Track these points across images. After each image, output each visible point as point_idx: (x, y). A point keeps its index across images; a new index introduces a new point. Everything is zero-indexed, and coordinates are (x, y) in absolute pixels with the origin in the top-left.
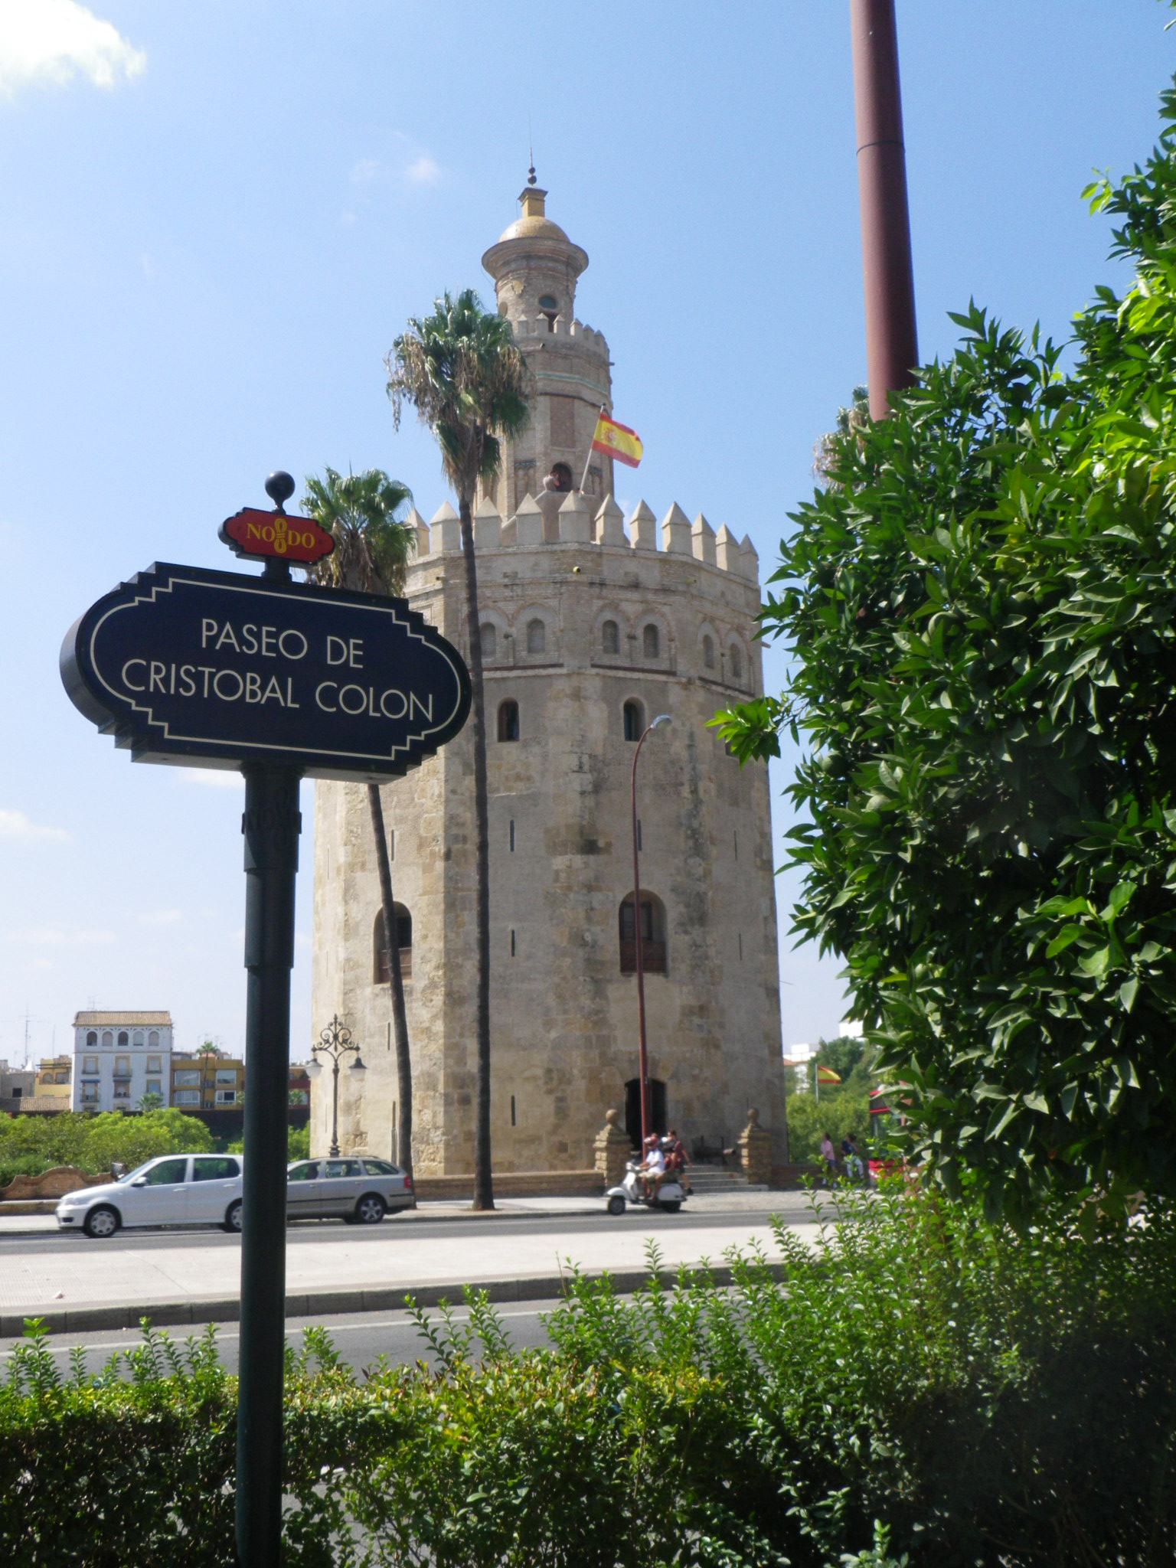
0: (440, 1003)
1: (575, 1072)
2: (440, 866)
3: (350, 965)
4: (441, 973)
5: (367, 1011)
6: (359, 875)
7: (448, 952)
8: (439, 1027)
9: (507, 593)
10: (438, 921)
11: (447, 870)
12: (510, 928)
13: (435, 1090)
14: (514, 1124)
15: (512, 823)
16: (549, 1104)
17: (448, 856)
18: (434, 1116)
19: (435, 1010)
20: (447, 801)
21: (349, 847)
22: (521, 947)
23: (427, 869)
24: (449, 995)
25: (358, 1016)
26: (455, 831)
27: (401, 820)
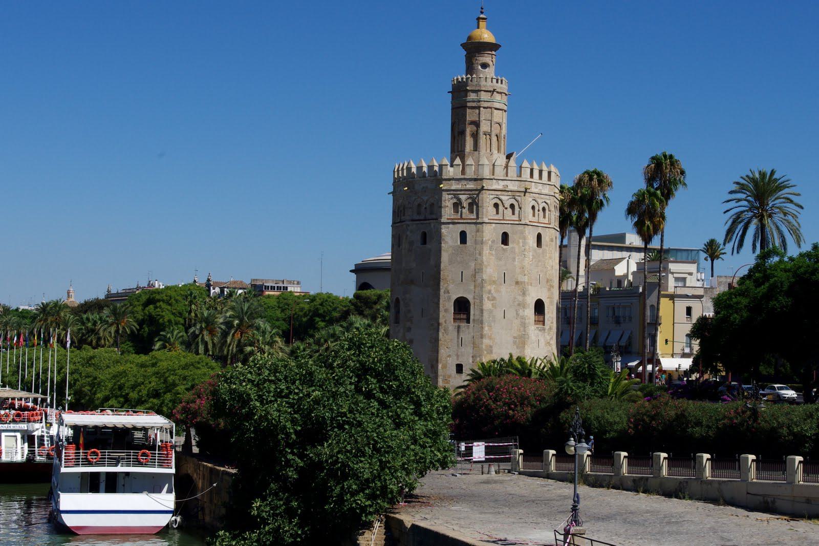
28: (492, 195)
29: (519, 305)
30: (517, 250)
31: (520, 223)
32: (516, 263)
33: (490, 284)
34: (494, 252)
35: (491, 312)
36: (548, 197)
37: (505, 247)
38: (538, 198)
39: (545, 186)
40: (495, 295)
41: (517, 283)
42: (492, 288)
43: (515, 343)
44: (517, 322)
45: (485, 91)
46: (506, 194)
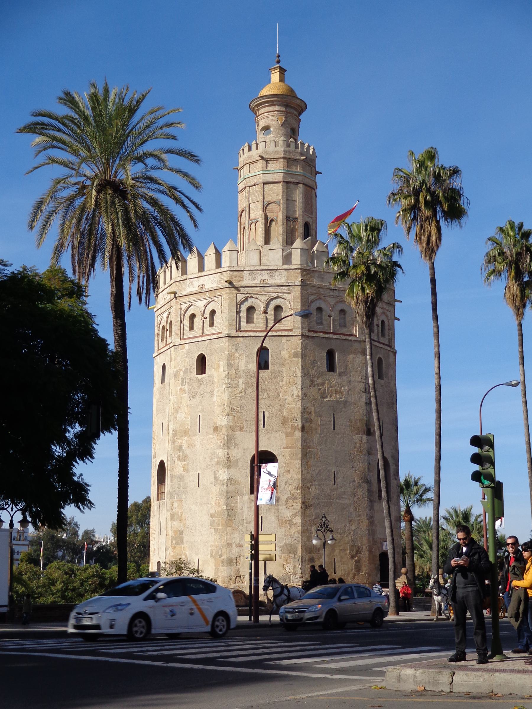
0: (299, 508)
1: (364, 547)
2: (298, 434)
3: (231, 482)
4: (299, 491)
5: (245, 509)
6: (238, 433)
7: (303, 480)
8: (298, 520)
9: (331, 293)
10: (297, 463)
11: (302, 436)
12: (333, 471)
13: (295, 553)
14: (335, 573)
15: (334, 415)
16: (351, 564)
17: (303, 429)
18: (295, 567)
19: (295, 511)
20: (302, 399)
21: (231, 418)
22: (338, 481)
23: (287, 435)
24: (303, 503)
25: (239, 511)
26: (306, 416)
27: (269, 406)
28: (186, 303)
29: (218, 463)
30: (216, 379)
31: (220, 335)
32: (215, 399)
33: (181, 436)
34: (186, 387)
35: (181, 478)
36: (285, 289)
37: (200, 377)
38: (259, 293)
39: (277, 273)
40: (187, 452)
41: (216, 429)
42: (184, 441)
43: (212, 524)
44: (216, 490)
45: (250, 163)
46: (203, 297)
